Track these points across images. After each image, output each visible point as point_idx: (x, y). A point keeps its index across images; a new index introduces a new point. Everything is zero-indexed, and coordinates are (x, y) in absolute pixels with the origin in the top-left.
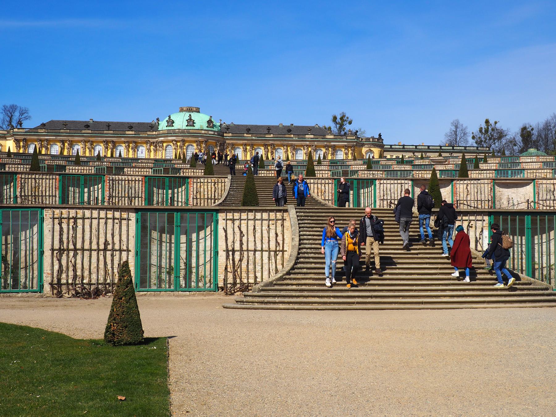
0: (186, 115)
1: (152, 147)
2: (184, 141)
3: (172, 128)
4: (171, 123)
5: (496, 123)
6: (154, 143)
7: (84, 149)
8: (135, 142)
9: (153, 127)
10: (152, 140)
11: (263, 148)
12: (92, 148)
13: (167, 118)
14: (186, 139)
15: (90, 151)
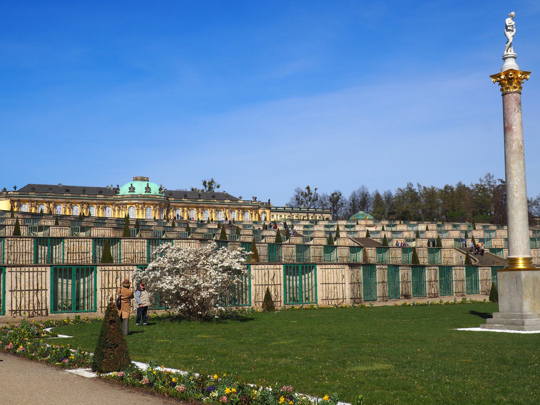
0: (144, 184)
1: (116, 208)
2: (144, 204)
3: (134, 193)
4: (132, 189)
5: (316, 189)
6: (118, 204)
7: (65, 208)
8: (105, 204)
9: (116, 191)
10: (117, 202)
11: (195, 209)
12: (71, 208)
13: (130, 186)
14: (146, 202)
15: (70, 210)
